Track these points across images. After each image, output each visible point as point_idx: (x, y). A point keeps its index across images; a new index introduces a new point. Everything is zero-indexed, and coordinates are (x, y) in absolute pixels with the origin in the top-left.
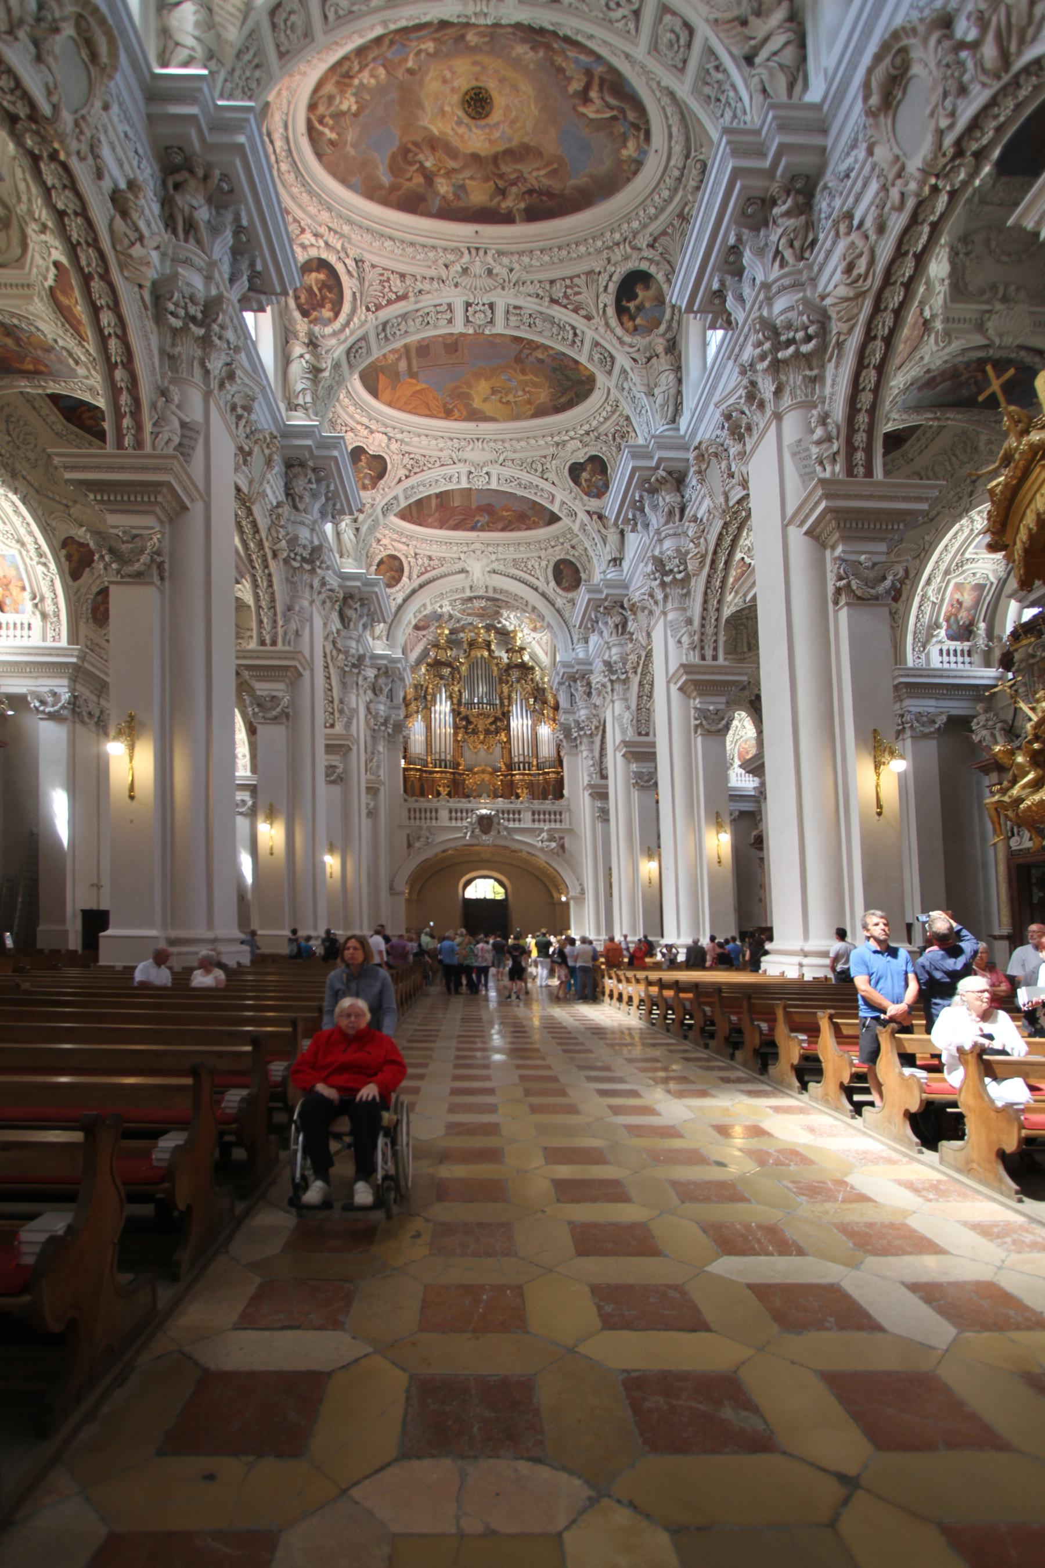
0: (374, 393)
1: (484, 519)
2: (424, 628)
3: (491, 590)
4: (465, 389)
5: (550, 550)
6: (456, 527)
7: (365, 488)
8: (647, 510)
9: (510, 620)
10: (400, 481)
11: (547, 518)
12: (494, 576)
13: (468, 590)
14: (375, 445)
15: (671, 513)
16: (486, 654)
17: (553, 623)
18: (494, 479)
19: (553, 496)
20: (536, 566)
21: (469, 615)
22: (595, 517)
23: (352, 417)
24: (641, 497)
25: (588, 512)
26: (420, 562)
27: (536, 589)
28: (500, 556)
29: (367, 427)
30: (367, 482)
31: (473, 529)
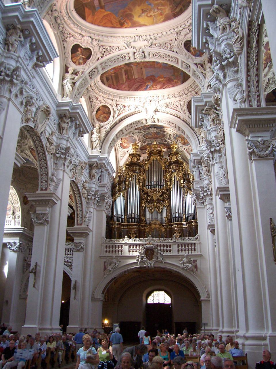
0: (83, 17)
1: (150, 84)
2: (127, 147)
4: (129, 12)
7: (80, 64)
8: (212, 32)
10: (98, 59)
11: (182, 79)
14: (85, 42)
15: (224, 29)
16: (158, 158)
17: (189, 135)
18: (147, 55)
19: (178, 59)
21: (150, 138)
22: (199, 66)
23: (72, 30)
24: (207, 25)
25: (196, 64)
26: (119, 108)
29: (80, 34)
30: (81, 61)
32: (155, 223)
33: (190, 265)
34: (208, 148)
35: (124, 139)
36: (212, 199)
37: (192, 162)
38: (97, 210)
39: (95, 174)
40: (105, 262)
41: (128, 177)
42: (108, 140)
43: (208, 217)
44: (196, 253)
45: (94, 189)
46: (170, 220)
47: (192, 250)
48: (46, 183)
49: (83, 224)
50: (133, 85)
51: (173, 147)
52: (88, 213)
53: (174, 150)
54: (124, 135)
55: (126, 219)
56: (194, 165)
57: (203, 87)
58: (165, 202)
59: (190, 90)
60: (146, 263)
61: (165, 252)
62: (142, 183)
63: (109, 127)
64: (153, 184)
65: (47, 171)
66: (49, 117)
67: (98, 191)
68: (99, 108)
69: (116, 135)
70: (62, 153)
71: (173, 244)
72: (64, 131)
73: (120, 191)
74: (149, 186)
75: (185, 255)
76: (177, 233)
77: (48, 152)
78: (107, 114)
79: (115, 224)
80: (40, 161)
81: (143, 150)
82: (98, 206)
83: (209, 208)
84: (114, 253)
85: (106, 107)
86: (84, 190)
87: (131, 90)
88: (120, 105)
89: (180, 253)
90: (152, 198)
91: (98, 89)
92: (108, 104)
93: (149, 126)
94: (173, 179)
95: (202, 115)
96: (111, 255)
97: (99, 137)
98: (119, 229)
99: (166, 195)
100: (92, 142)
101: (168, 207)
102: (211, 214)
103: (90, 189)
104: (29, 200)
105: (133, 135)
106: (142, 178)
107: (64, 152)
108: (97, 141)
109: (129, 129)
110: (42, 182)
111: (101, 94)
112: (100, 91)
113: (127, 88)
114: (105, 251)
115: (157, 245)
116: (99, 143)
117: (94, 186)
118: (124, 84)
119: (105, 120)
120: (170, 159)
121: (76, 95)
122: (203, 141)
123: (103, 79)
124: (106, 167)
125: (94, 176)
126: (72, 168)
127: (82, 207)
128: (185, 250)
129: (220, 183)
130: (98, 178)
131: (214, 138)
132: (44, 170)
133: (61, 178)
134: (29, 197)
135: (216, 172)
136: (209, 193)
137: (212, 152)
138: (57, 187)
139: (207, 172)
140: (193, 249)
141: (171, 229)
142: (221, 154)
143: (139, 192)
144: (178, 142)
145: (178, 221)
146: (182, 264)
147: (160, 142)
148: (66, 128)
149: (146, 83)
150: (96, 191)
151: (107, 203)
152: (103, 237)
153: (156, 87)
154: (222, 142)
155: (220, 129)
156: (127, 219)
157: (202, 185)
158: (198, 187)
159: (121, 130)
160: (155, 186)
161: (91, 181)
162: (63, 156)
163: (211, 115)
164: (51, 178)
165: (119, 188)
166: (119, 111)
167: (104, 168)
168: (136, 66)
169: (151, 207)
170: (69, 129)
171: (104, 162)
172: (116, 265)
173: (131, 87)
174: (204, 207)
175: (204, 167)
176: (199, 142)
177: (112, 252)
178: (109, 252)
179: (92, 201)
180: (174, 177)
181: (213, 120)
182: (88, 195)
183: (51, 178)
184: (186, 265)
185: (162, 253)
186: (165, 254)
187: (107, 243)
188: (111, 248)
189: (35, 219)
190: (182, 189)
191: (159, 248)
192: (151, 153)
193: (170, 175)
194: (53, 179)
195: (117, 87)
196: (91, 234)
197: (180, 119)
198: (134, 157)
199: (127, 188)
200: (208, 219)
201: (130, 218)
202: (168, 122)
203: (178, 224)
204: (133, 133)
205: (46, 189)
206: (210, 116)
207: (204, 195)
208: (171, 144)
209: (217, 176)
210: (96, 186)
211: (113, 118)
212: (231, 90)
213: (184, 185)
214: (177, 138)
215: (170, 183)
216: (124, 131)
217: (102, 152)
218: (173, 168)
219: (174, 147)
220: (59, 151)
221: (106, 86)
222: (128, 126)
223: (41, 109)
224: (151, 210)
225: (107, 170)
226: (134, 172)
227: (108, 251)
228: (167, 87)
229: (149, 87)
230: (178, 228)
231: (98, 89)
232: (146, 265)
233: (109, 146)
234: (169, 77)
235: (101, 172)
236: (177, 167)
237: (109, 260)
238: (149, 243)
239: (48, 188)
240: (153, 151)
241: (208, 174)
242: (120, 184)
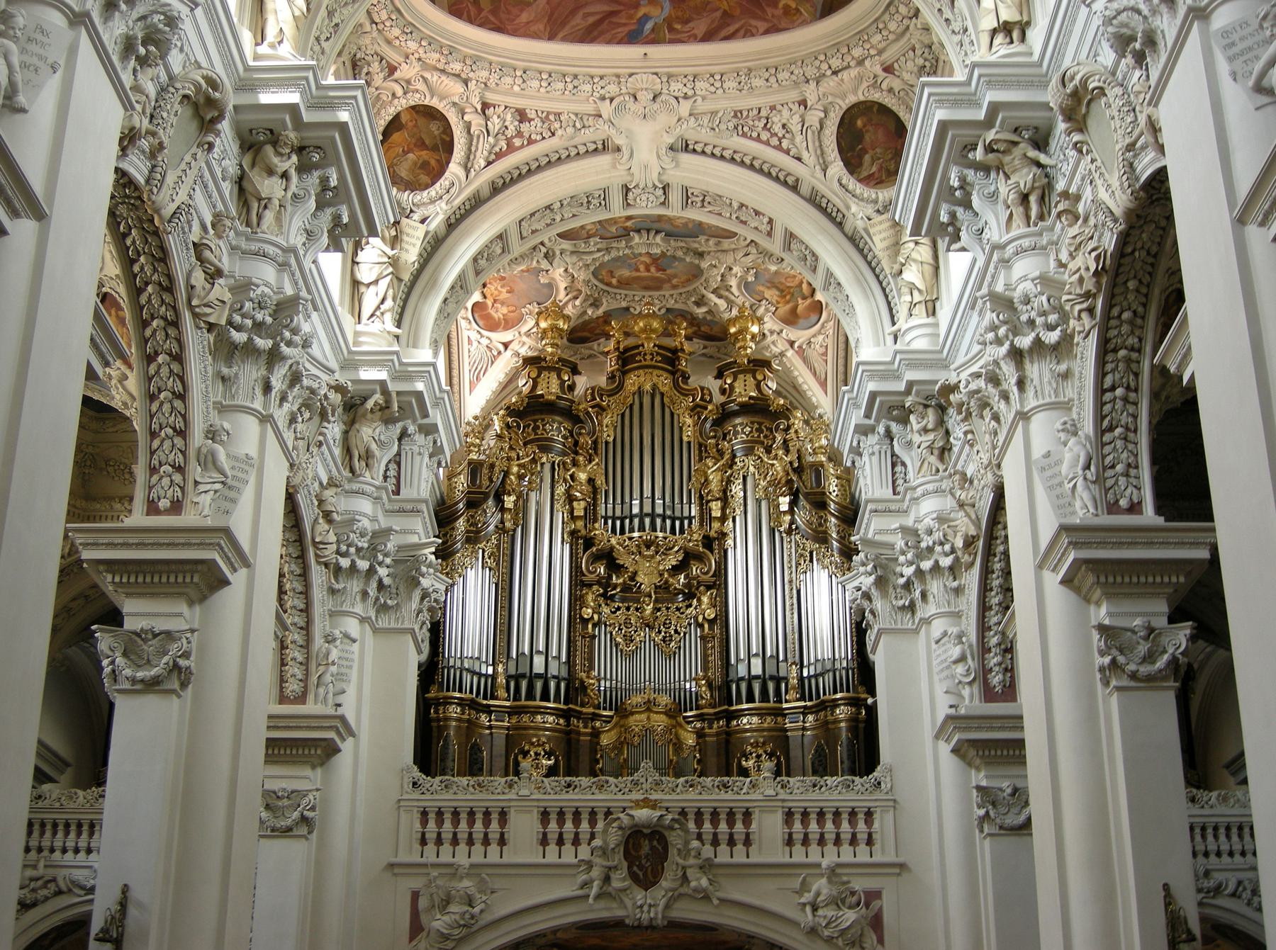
2: (508, 324)
3: (675, 197)
5: (830, 83)
6: (588, 36)
9: (728, 289)
12: (685, 158)
13: (616, 199)
17: (842, 273)
20: (795, 128)
21: (624, 284)
26: (495, 125)
27: (794, 188)
28: (702, 106)
31: (632, 38)
32: (649, 706)
33: (849, 916)
34: (1002, 331)
35: (498, 285)
36: (958, 591)
37: (857, 406)
38: (376, 631)
39: (374, 446)
40: (415, 896)
41: (515, 469)
42: (433, 283)
43: (936, 678)
44: (878, 858)
45: (365, 523)
46: (720, 688)
47: (854, 841)
48: (177, 478)
49: (311, 697)
50: (573, 12)
51: (740, 332)
52: (335, 640)
53: (745, 349)
54: (508, 258)
55: (501, 680)
56: (867, 422)
57: (957, 38)
58: (699, 600)
59: (857, 52)
60: (626, 900)
61: (723, 848)
62: (583, 504)
63: (441, 217)
64: (636, 510)
65: (184, 417)
66: (210, 139)
67: (388, 532)
68: (397, 117)
69: (475, 260)
70: (258, 326)
71: (763, 810)
72: (269, 216)
73: (473, 538)
74: (614, 519)
75: (825, 863)
76: (759, 756)
77: (196, 316)
78: (435, 149)
79: (447, 702)
80: (150, 359)
81: (583, 340)
82: (383, 609)
83: (945, 634)
84: (462, 848)
85: (430, 114)
86: (323, 525)
87: (561, 35)
88: (500, 110)
89: (799, 855)
90: (632, 578)
91: (401, 22)
92: (442, 98)
93: (629, 224)
94: (737, 489)
95: (966, 171)
96: (446, 855)
97: (394, 262)
98: (472, 725)
99: (702, 567)
100: (356, 283)
101: (711, 628)
102: (956, 662)
103: (352, 521)
104: (88, 561)
105: (545, 264)
106: (583, 476)
107: (269, 320)
108: (384, 283)
109: (533, 232)
110: (153, 470)
111: (412, 45)
112: (410, 29)
113: (541, 27)
114: (419, 835)
115: (683, 813)
116: (391, 292)
117: (365, 506)
119: (424, 178)
120: (723, 391)
121: (318, 39)
122: (913, 305)
124: (426, 415)
125: (368, 456)
126: (295, 408)
127: (307, 610)
128: (822, 841)
129: (1062, 503)
130: (383, 468)
131: (1028, 286)
132: (166, 407)
133: (253, 451)
134: (85, 545)
135: (1037, 453)
136: (946, 562)
137: (1017, 355)
138: (234, 501)
139: (933, 459)
140: (862, 837)
141: (728, 734)
142: (1063, 367)
143: (567, 547)
144: (761, 311)
145: (765, 696)
146: (808, 909)
147: (671, 304)
148: (277, 203)
150: (375, 534)
151: (425, 595)
152: (408, 770)
153: (687, 28)
154: (1085, 305)
155: (1078, 240)
156: (508, 678)
157: (909, 522)
158: (886, 532)
159: (500, 237)
160: (647, 521)
161: (350, 481)
162: (263, 343)
163: (1013, 172)
164: (204, 450)
165: (472, 522)
166: (491, 139)
167: (414, 421)
169: (627, 623)
170: (289, 208)
171: (420, 386)
172: (477, 910)
174: (916, 631)
175: (919, 432)
176: (891, 309)
177: (455, 841)
178: (455, 841)
179: (355, 586)
180: (745, 478)
181: (1024, 199)
182: (338, 552)
183: (204, 450)
184: (830, 912)
185: (708, 851)
186: (723, 855)
187: (428, 796)
188: (447, 825)
189: (120, 661)
190: (782, 538)
191: (691, 825)
192: (627, 359)
193: (722, 470)
194: (213, 454)
195: (492, 19)
196: (347, 746)
197: (798, 193)
198: (545, 374)
199: (508, 525)
200: (940, 689)
201: (523, 676)
202: (735, 205)
203: (760, 713)
204: (548, 256)
205: (176, 507)
206: (1007, 177)
207: (919, 573)
208: (726, 316)
209: (1048, 473)
210: (375, 510)
211: (462, 173)
212: (1235, 37)
213: (792, 522)
214: (761, 288)
215: (723, 509)
216: (514, 238)
217: (403, 340)
218: (736, 433)
219: (743, 331)
220: (244, 316)
222: (532, 215)
223: (181, 92)
224: (629, 639)
225: (429, 430)
226: (545, 449)
227: (431, 836)
228: (742, 32)
229: (649, 26)
230: (763, 730)
231: (401, 22)
232: (625, 907)
233: (440, 311)
235: (400, 440)
236: (759, 430)
237: (439, 882)
238: (646, 803)
239: (187, 505)
240: (637, 347)
241: (941, 467)
242: (474, 503)
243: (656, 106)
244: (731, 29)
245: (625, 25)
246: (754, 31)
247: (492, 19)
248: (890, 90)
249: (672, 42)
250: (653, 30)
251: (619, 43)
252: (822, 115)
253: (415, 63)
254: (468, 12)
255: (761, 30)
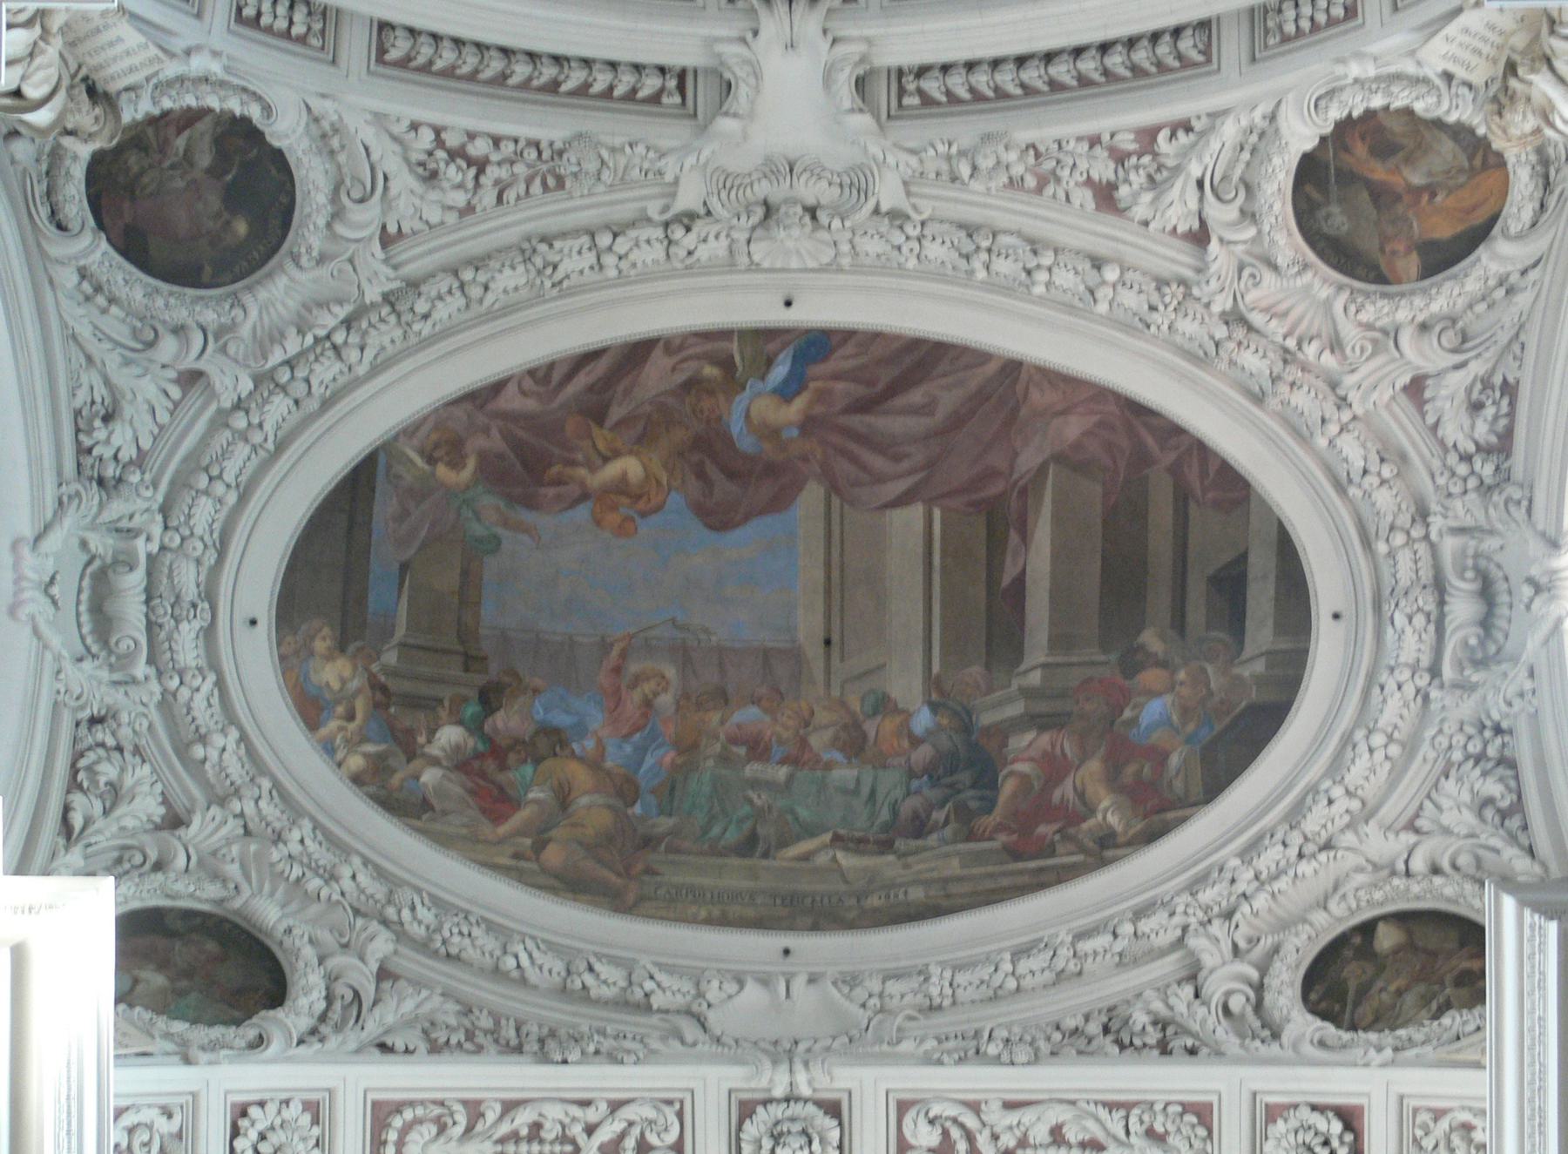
1: (758, 410)
6: (924, 358)
11: (385, 506)
31: (818, 344)
50: (957, 421)
85: (1343, 256)
87: (991, 368)
111: (1353, 451)
113: (1035, 396)
118: (1058, 458)
123: (1280, 629)
149: (808, 425)
168: (883, 705)
173: (981, 396)
195: (1150, 441)
221: (1267, 509)
228: (556, 376)
229: (780, 371)
234: (527, 516)
243: (763, 189)
244: (582, 380)
245: (837, 377)
246: (528, 384)
247: (1150, 441)
248: (179, 330)
249: (725, 334)
250: (770, 362)
251: (848, 335)
252: (340, 229)
253: (1353, 396)
254: (1203, 474)
255: (512, 388)
